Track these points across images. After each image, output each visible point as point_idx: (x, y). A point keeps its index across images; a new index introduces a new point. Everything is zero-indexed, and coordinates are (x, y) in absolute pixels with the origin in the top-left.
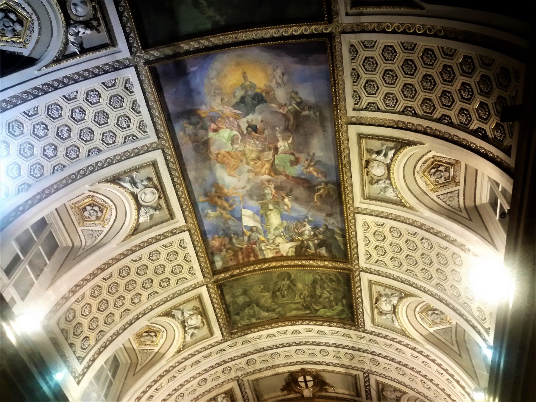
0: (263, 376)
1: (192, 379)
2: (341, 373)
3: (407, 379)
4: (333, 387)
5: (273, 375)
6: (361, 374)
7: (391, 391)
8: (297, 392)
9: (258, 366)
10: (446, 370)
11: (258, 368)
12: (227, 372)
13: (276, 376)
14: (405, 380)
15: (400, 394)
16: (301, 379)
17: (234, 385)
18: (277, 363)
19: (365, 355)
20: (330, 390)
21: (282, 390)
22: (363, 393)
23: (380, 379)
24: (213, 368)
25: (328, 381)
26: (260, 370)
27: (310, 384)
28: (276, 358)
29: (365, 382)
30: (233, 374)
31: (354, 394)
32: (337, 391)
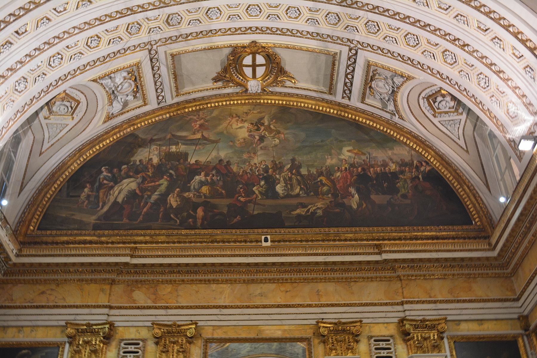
0: (190, 48)
1: (77, 31)
2: (313, 51)
3: (420, 53)
4: (293, 78)
5: (205, 49)
6: (345, 50)
7: (386, 79)
8: (238, 84)
9: (185, 29)
10: (498, 20)
11: (184, 32)
12: (134, 30)
13: (210, 53)
14: (416, 55)
15: (402, 80)
16: (248, 60)
17: (142, 56)
18: (215, 26)
19: (361, 13)
20: (288, 84)
21: (216, 80)
22: (340, 87)
23: (374, 58)
24: (110, 17)
25: (287, 68)
26: (187, 37)
27: (260, 71)
28: (214, 18)
29: (348, 67)
30: (143, 37)
31: (325, 90)
32: (299, 85)
